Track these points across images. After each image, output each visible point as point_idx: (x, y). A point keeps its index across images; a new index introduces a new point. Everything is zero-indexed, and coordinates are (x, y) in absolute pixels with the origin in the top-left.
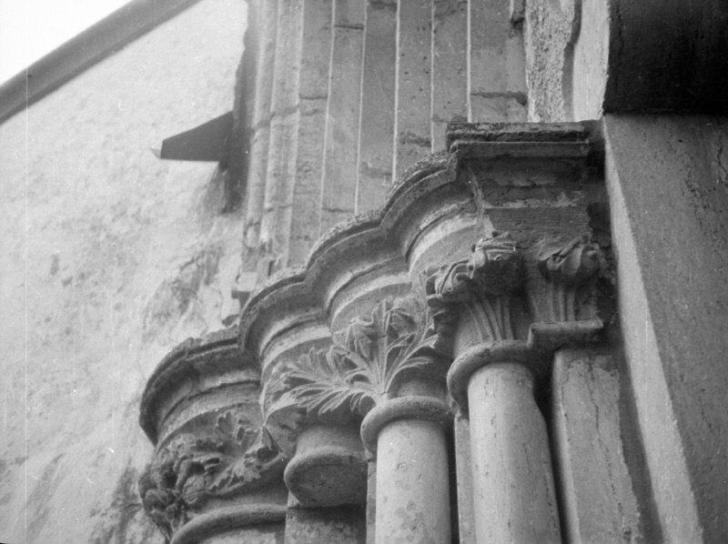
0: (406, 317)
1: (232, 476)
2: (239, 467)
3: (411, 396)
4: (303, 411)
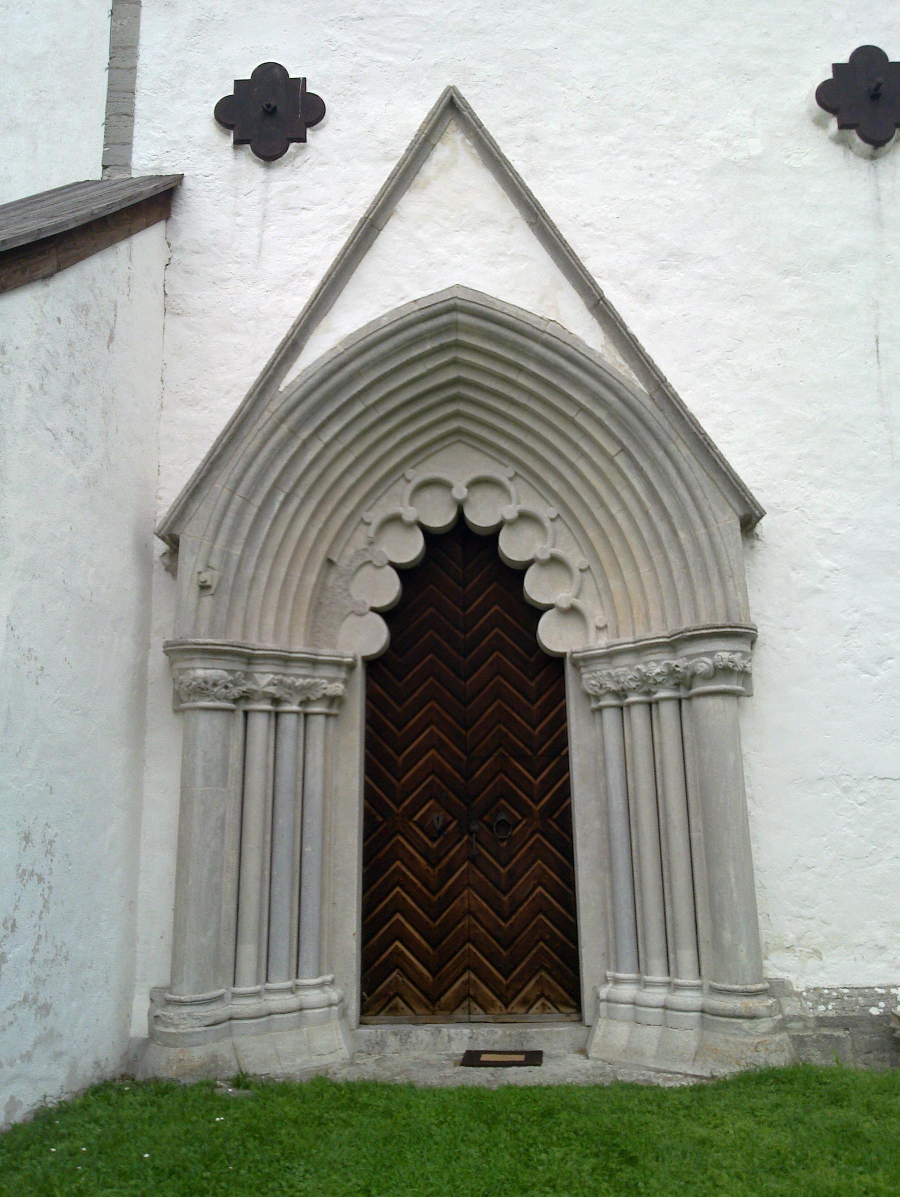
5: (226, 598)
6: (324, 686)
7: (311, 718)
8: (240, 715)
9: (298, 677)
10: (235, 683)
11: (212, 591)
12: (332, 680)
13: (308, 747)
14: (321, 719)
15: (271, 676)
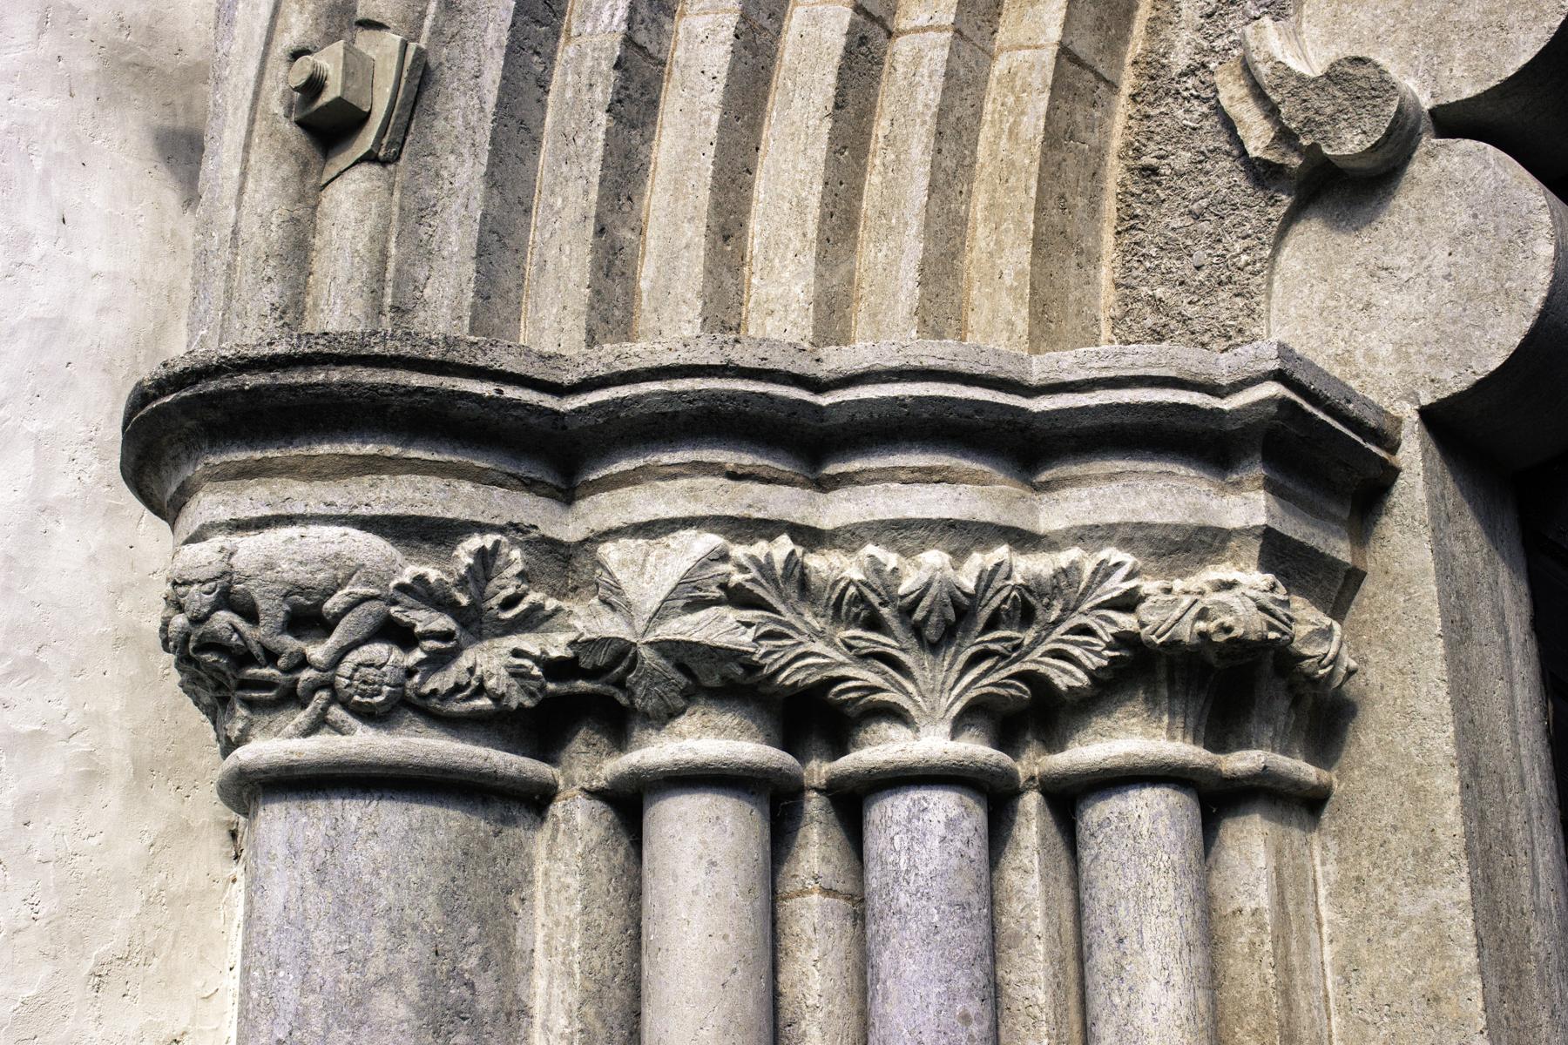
0: (1025, 601)
1: (474, 683)
2: (489, 660)
3: (975, 749)
4: (753, 668)
5: (465, 174)
6: (1116, 586)
7: (1099, 813)
8: (578, 820)
9: (897, 520)
10: (475, 623)
11: (366, 140)
12: (1197, 544)
13: (1097, 1003)
14: (1153, 815)
15: (710, 541)
